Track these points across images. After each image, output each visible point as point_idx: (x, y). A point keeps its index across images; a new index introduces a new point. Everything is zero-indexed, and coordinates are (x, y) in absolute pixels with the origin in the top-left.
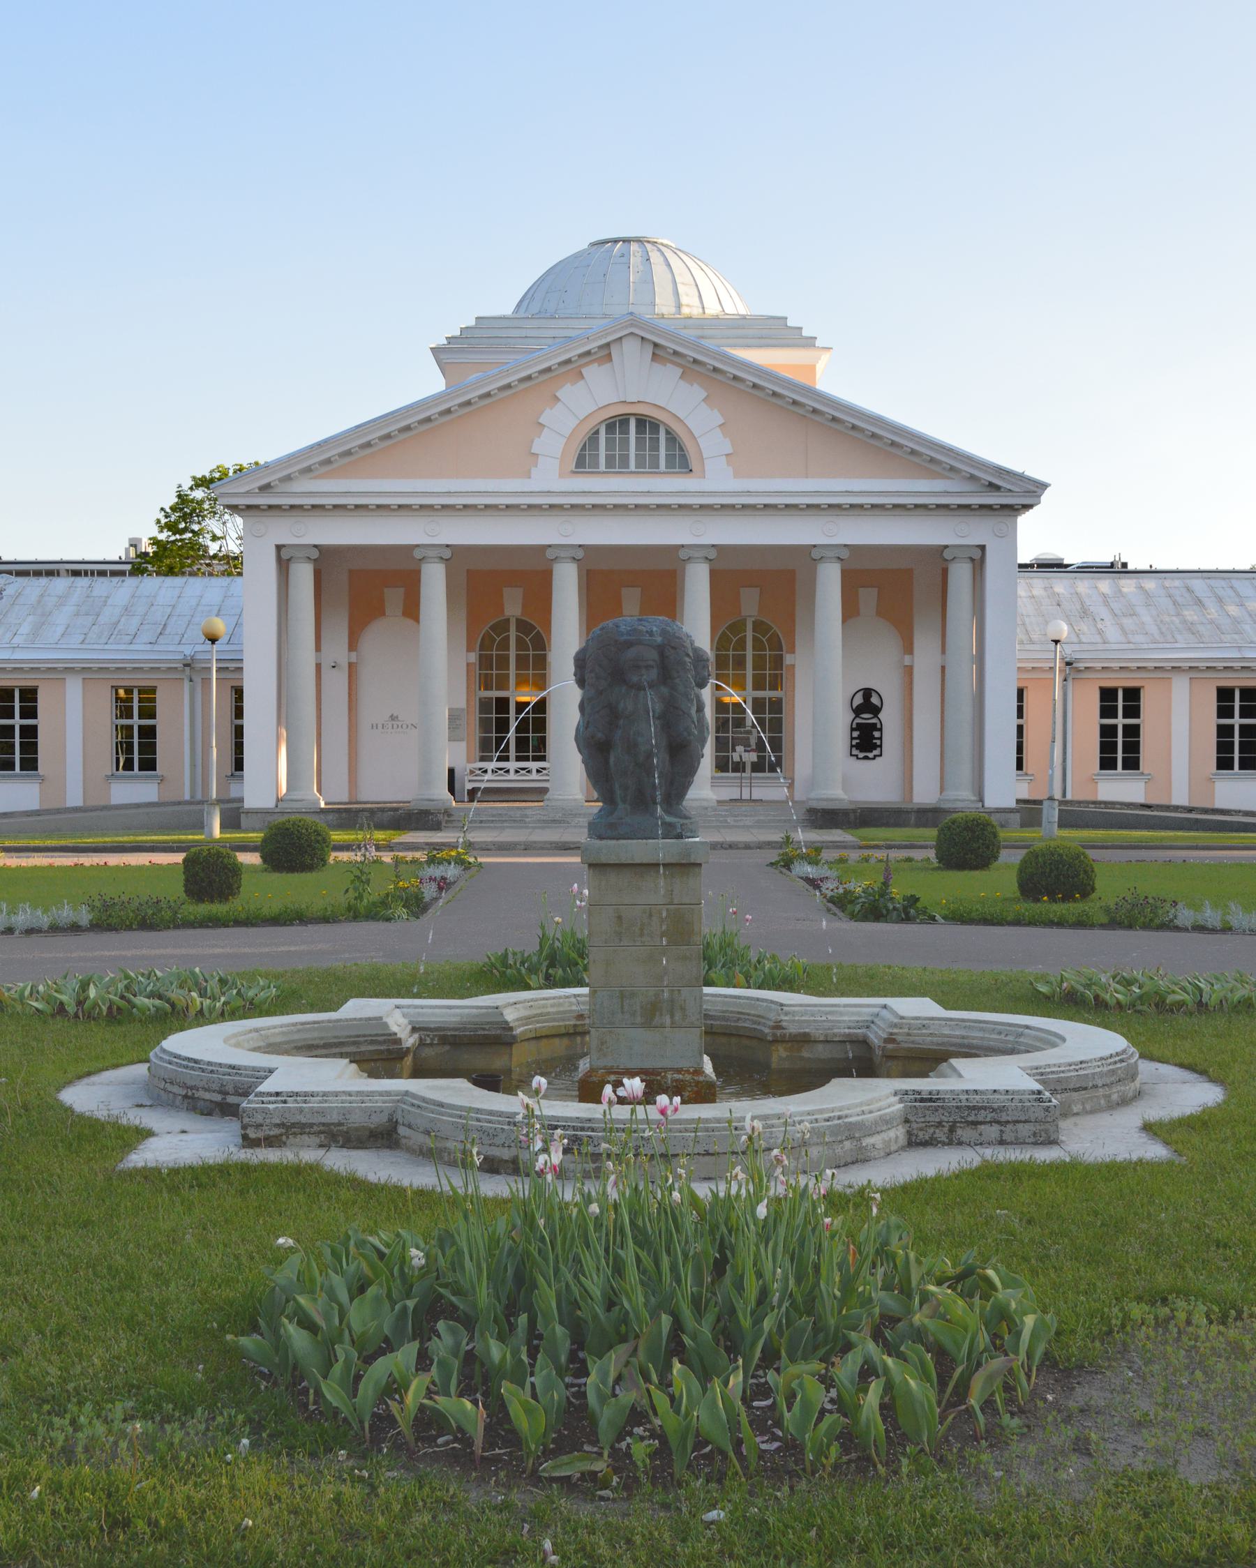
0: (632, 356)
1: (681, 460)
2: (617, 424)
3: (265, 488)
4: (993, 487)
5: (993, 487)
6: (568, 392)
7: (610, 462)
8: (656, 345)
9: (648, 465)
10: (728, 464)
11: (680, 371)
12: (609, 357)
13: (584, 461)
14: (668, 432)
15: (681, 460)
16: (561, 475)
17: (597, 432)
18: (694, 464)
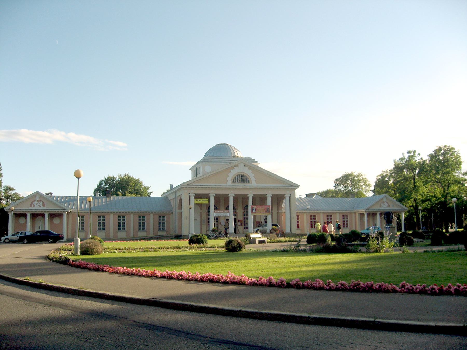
0: (241, 165)
1: (248, 181)
2: (238, 176)
3: (188, 185)
4: (292, 186)
5: (292, 186)
6: (232, 171)
7: (238, 181)
8: (245, 164)
9: (243, 181)
10: (255, 182)
11: (248, 168)
12: (238, 166)
13: (234, 182)
14: (246, 177)
15: (248, 181)
16: (231, 183)
17: (236, 177)
18: (250, 182)
